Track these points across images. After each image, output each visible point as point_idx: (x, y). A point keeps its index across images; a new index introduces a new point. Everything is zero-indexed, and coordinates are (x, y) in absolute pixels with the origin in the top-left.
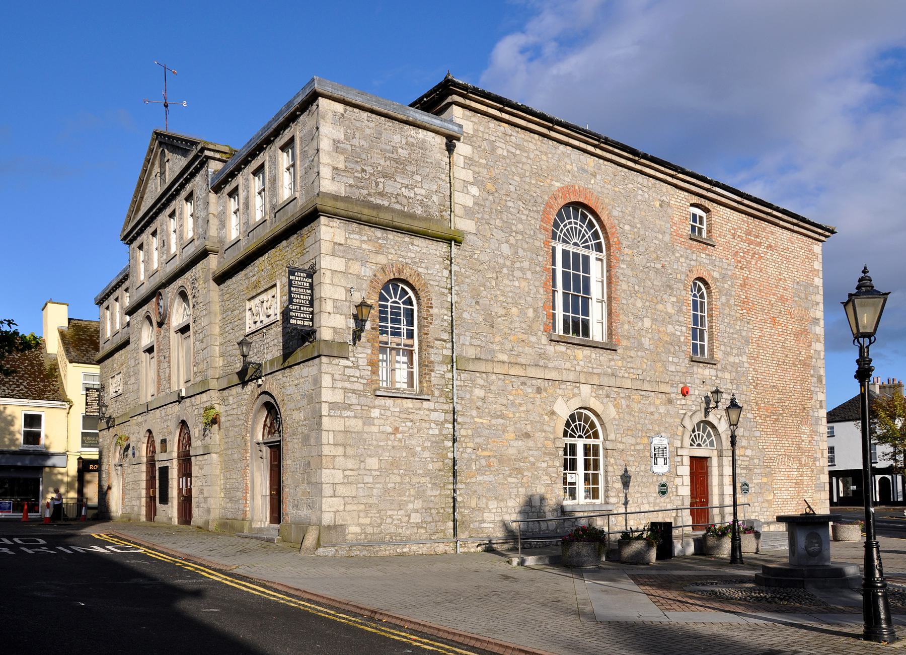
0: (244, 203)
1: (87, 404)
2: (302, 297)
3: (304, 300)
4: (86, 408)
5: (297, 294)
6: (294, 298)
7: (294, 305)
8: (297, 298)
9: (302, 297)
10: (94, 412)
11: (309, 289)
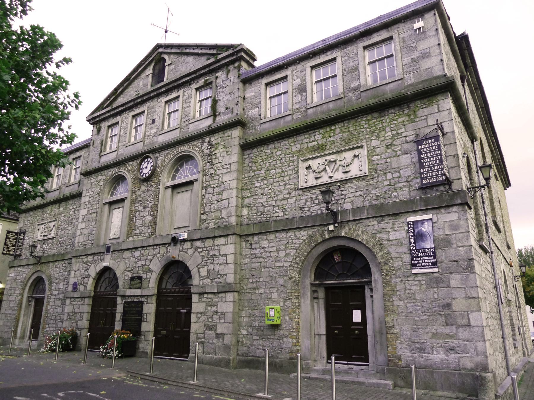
0: (193, 49)
1: (5, 244)
2: (432, 159)
3: (434, 161)
4: (4, 248)
5: (427, 158)
6: (424, 162)
7: (425, 168)
8: (428, 161)
9: (432, 159)
10: (10, 251)
11: (438, 151)
